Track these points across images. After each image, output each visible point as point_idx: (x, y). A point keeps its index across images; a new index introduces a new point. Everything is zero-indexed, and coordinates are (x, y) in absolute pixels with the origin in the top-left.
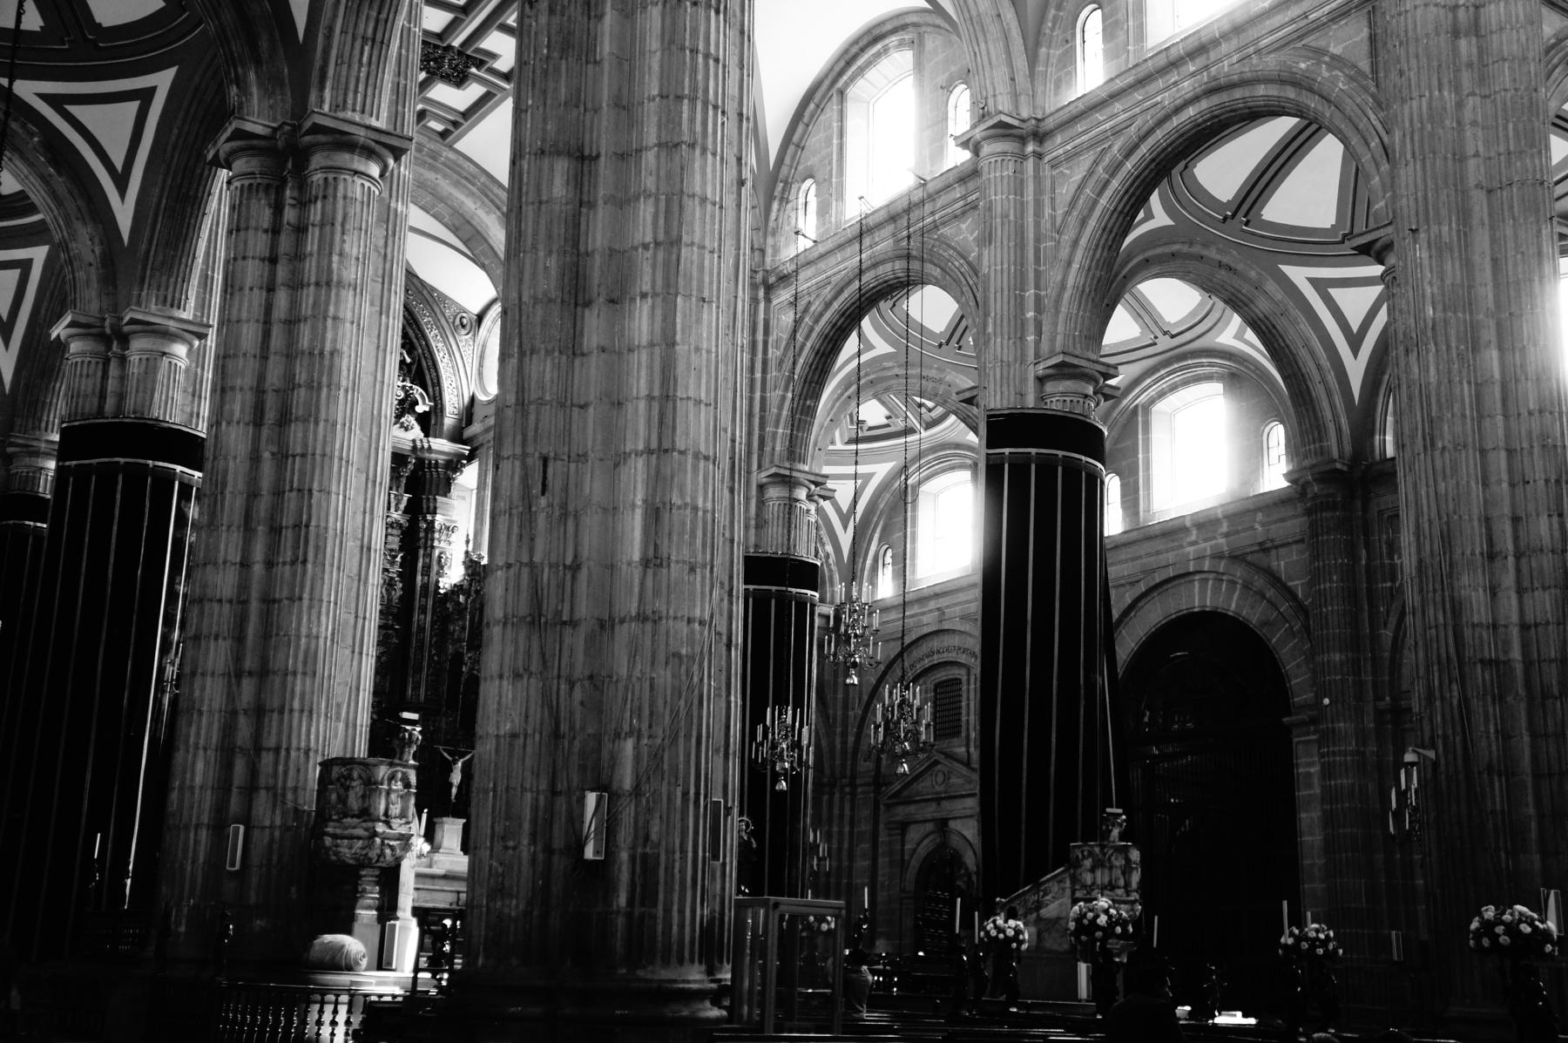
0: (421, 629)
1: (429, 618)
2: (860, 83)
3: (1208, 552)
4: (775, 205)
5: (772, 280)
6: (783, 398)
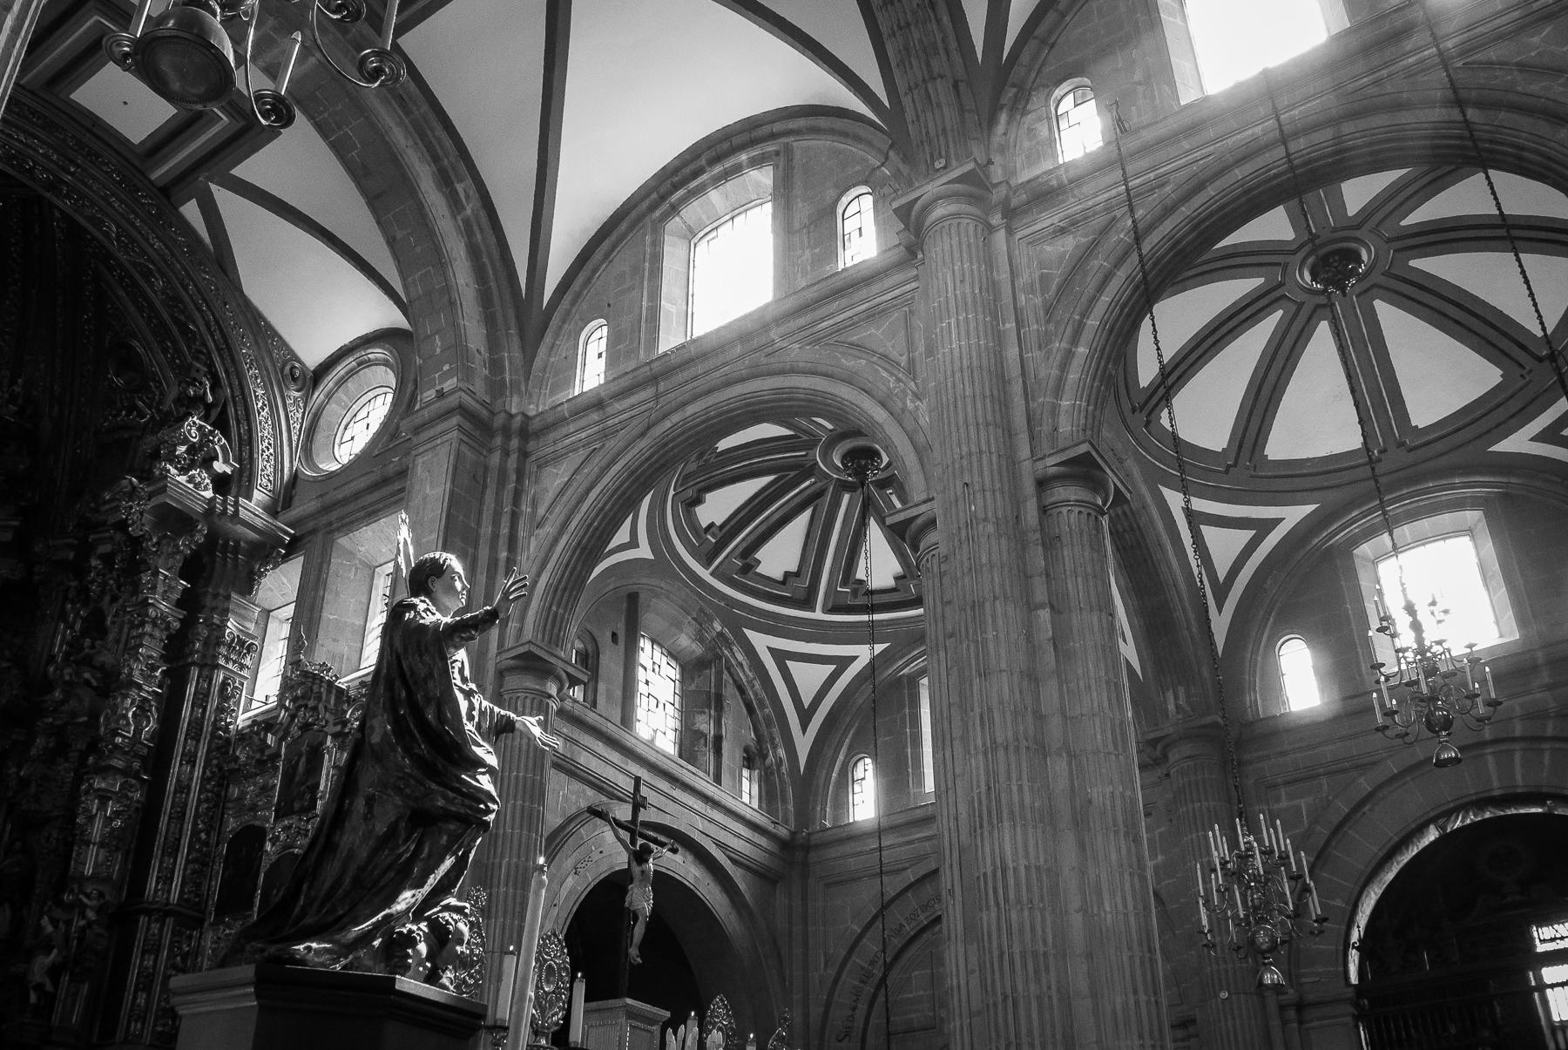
1: (198, 773)
3: (1518, 711)
6: (1069, 355)
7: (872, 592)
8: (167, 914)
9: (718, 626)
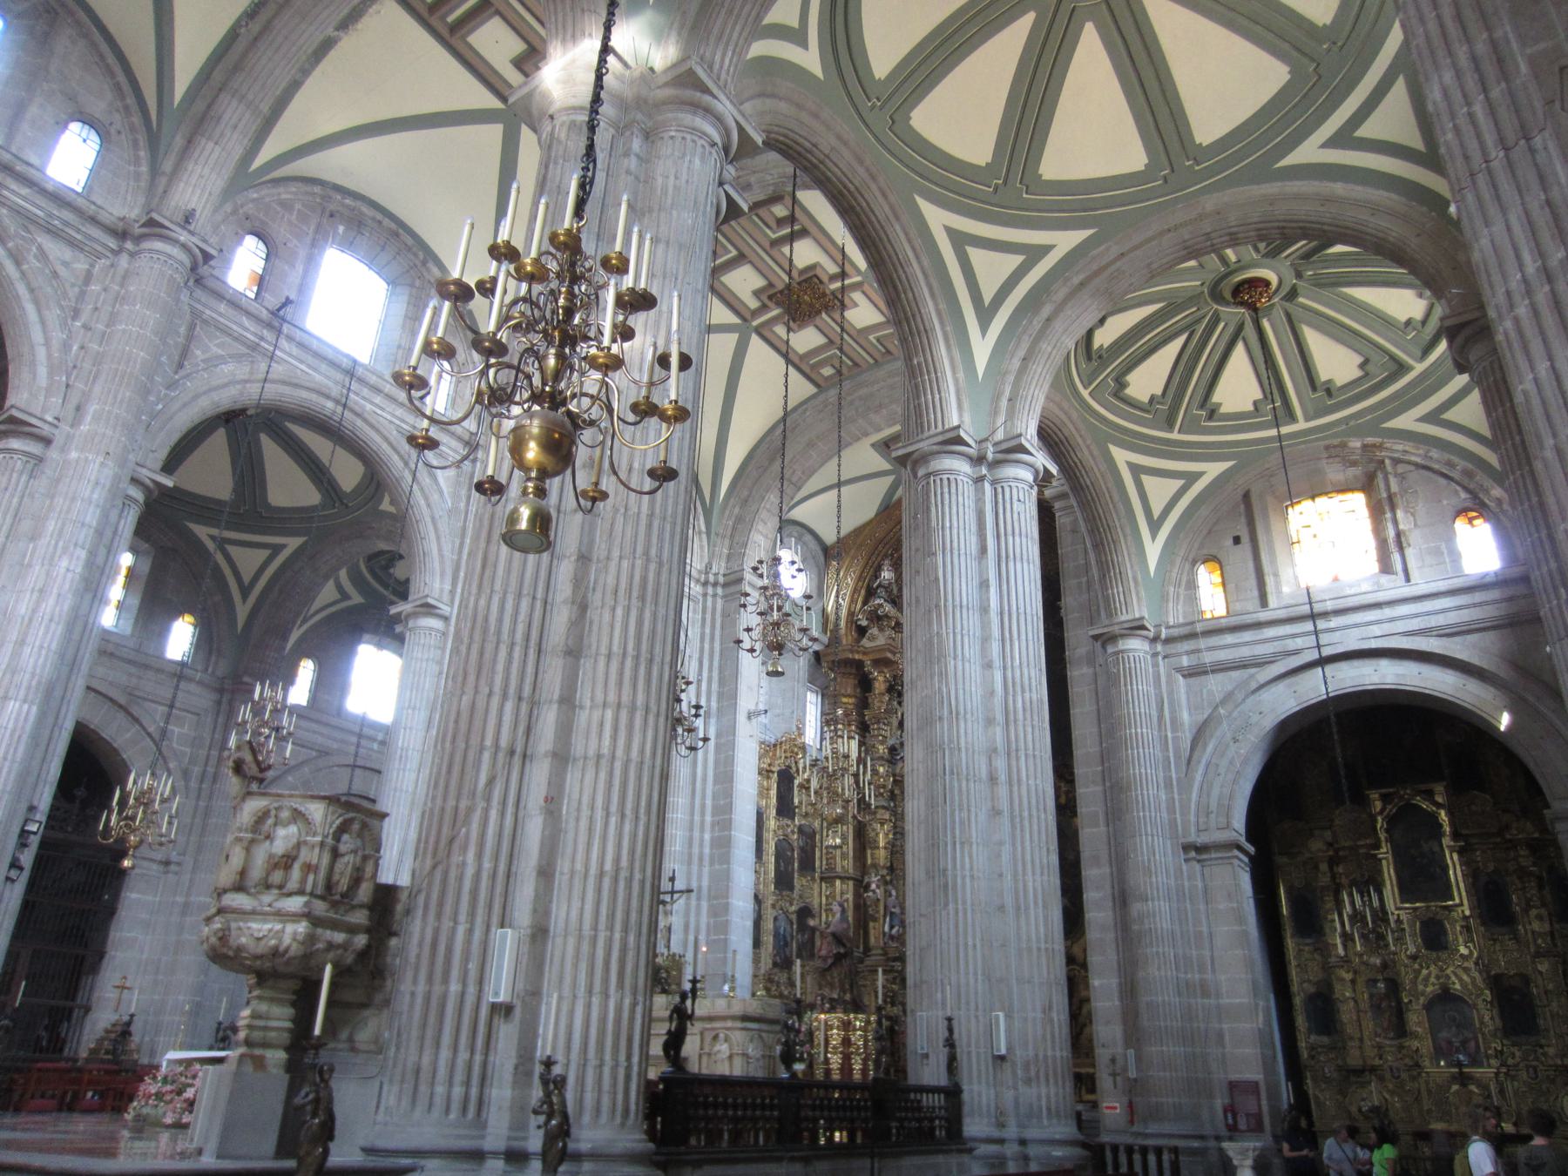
7: (1424, 322)
9: (1356, 444)
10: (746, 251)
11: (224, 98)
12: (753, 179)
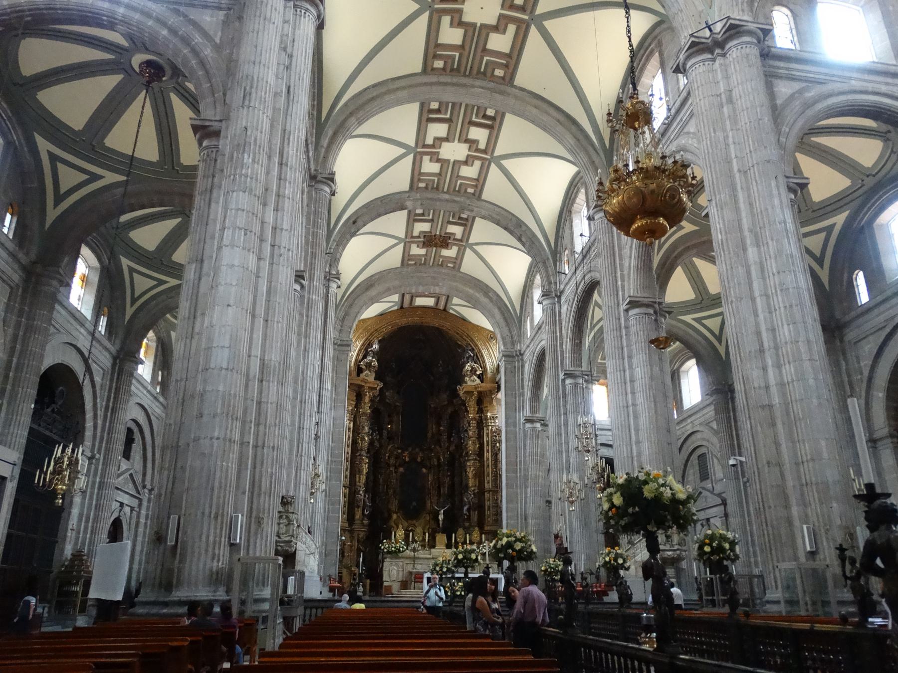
0: (488, 459)
2: (575, 205)
4: (558, 264)
5: (559, 294)
8: (490, 491)
10: (436, 220)
11: (353, 120)
12: (476, 209)
